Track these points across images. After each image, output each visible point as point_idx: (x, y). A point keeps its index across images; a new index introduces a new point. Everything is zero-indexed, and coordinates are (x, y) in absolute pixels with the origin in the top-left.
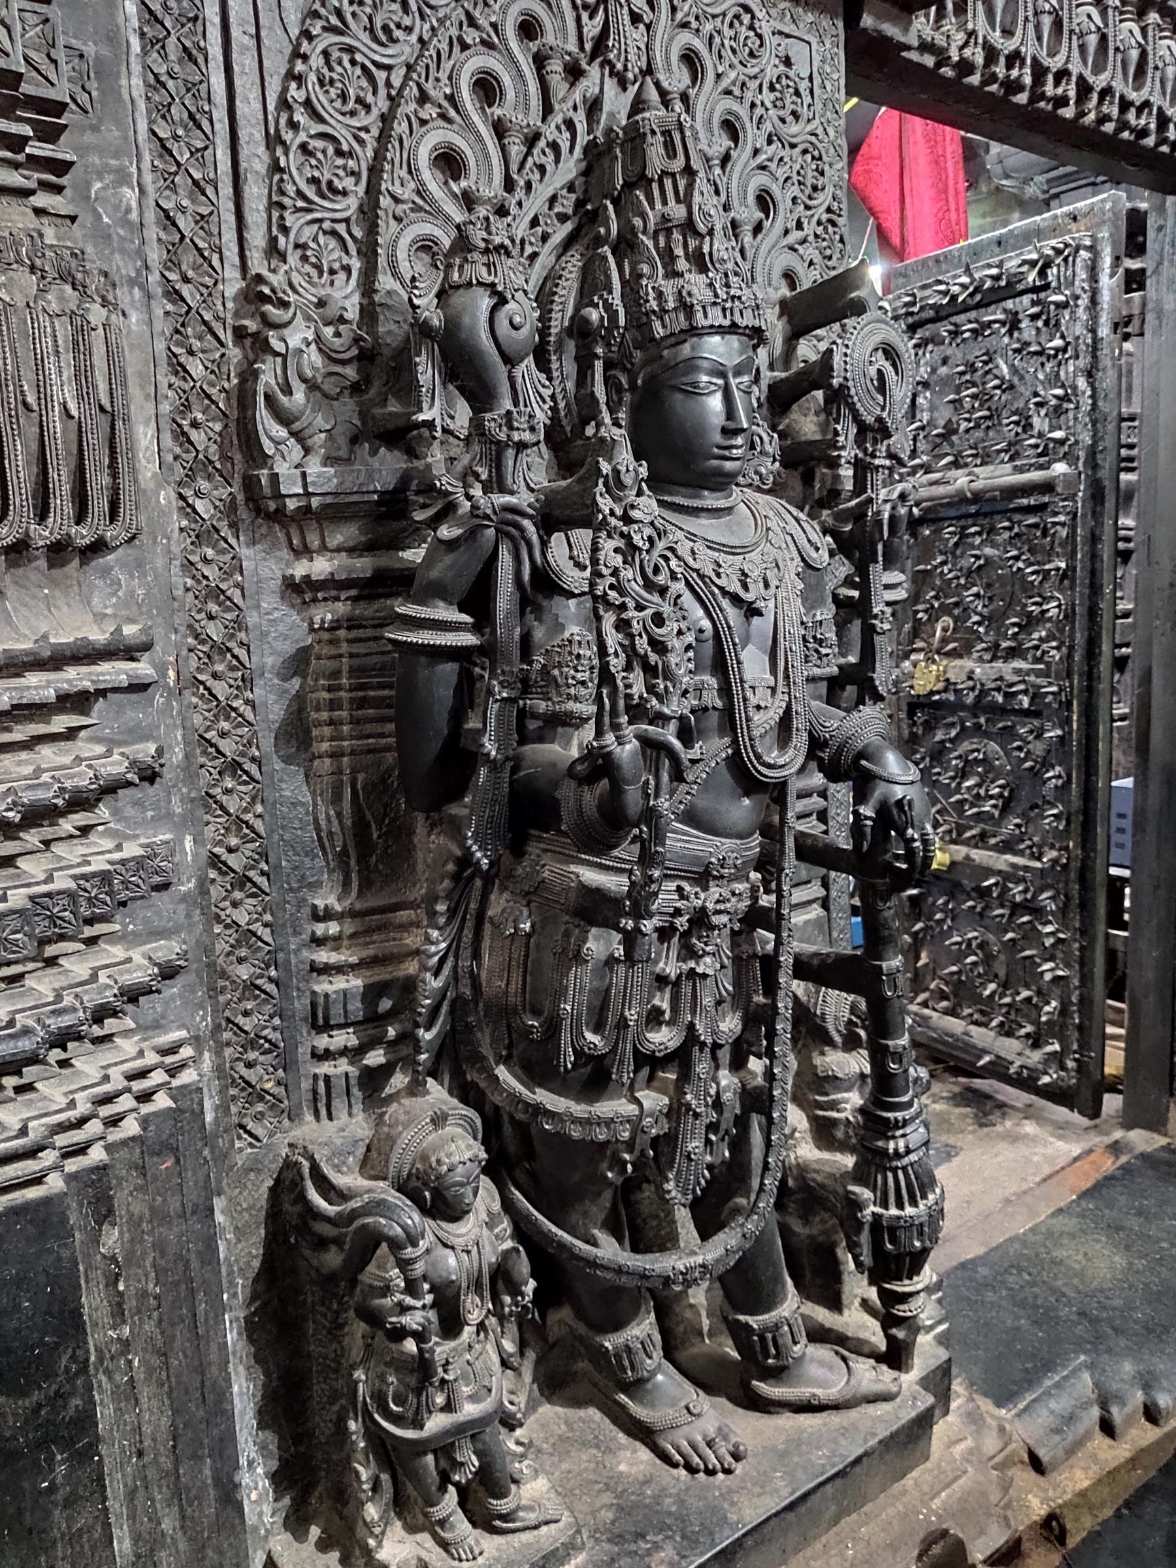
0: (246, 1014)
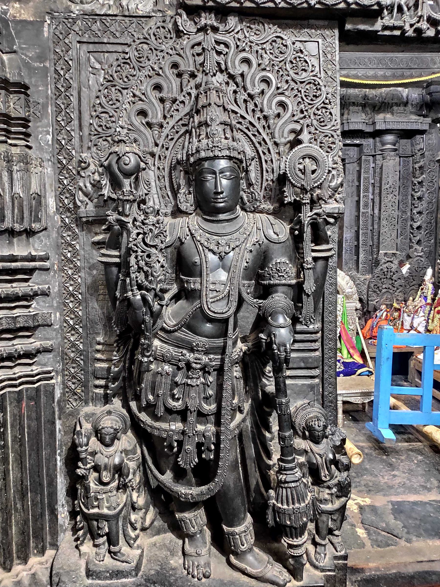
0: (73, 368)
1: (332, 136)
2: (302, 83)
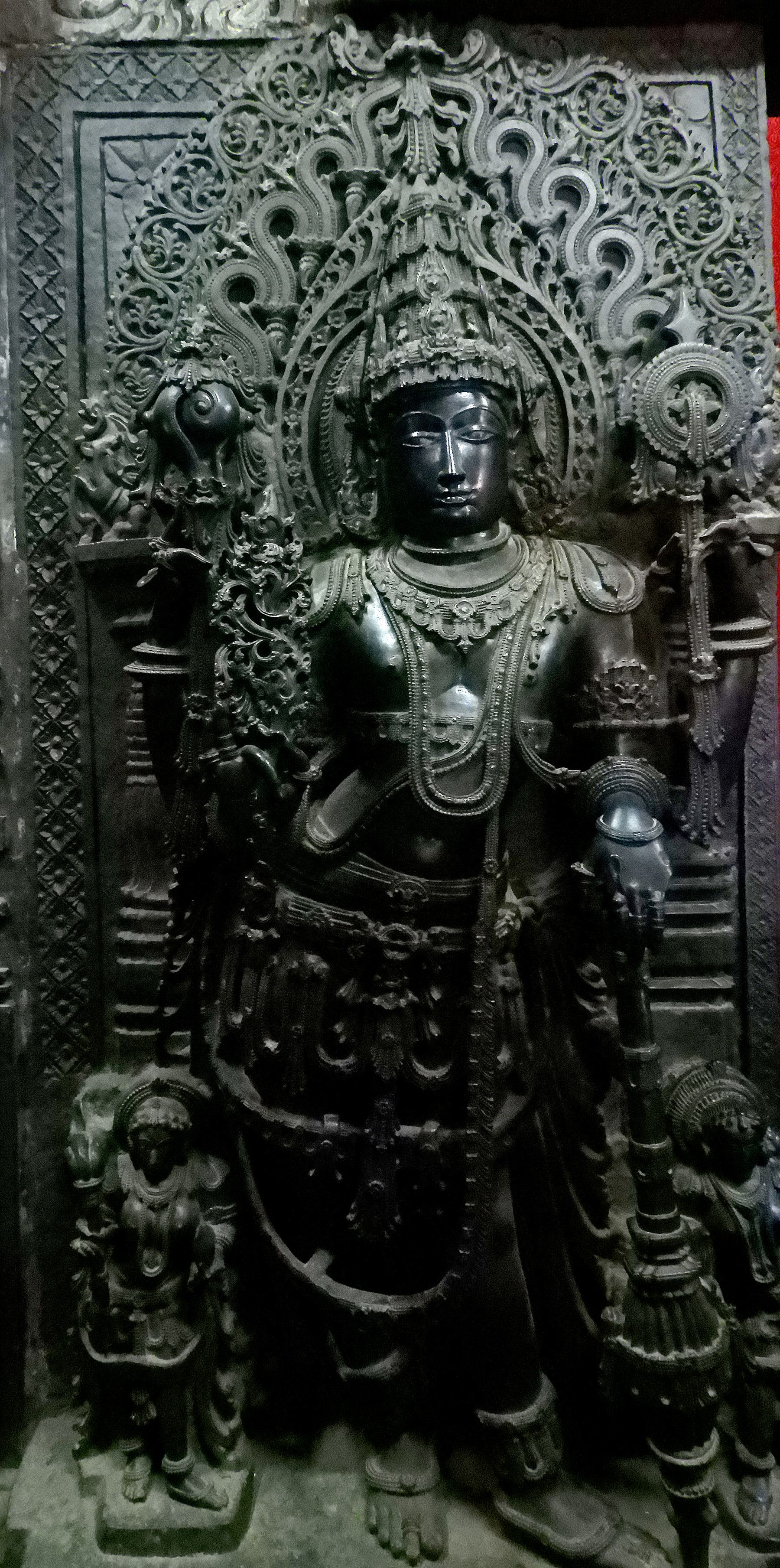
1: (755, 331)
2: (667, 192)
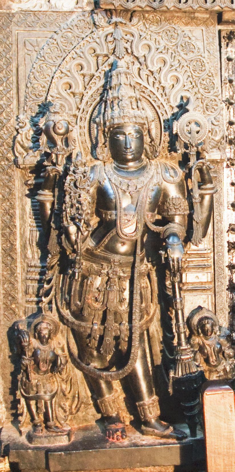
1: (215, 100)
